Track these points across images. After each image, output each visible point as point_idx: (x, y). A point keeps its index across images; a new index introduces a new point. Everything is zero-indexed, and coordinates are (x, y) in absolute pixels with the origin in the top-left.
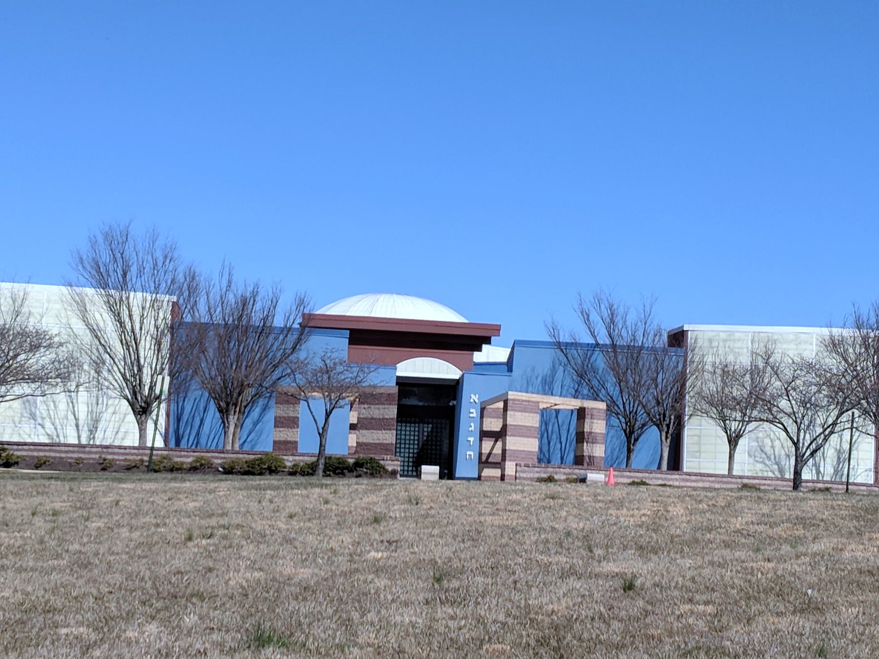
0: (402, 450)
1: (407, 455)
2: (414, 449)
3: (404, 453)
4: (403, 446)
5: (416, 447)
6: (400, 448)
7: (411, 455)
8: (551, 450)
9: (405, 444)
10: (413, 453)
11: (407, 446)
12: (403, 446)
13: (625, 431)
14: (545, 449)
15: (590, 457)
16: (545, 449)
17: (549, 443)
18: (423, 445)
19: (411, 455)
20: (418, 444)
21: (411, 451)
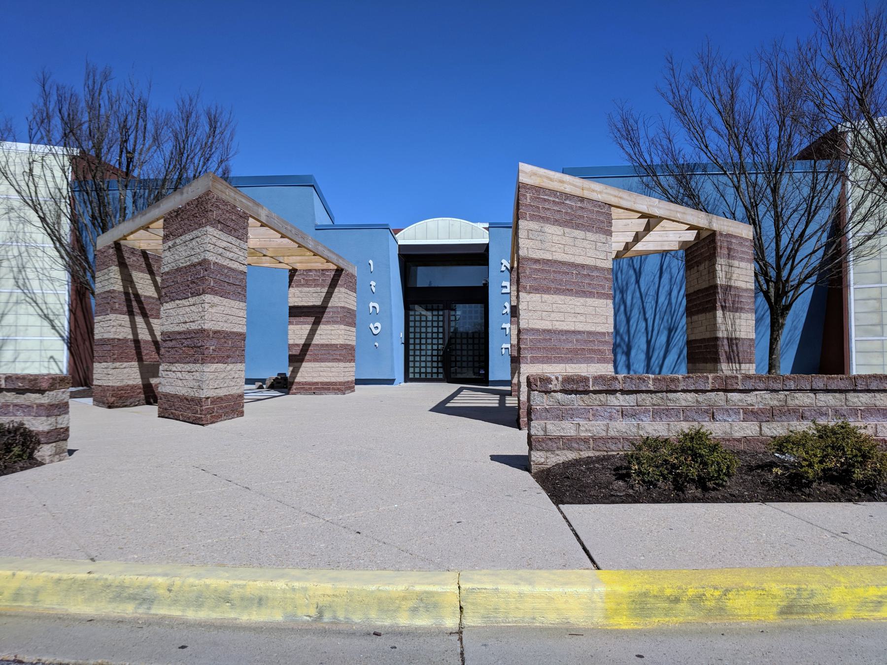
0: (423, 347)
1: (429, 353)
2: (438, 344)
3: (427, 350)
4: (423, 341)
5: (441, 341)
6: (420, 344)
7: (435, 353)
8: (632, 332)
9: (426, 338)
10: (438, 350)
11: (429, 341)
12: (423, 341)
13: (766, 294)
14: (623, 329)
15: (730, 340)
16: (623, 329)
17: (628, 321)
18: (450, 339)
19: (435, 353)
20: (443, 338)
21: (435, 347)
